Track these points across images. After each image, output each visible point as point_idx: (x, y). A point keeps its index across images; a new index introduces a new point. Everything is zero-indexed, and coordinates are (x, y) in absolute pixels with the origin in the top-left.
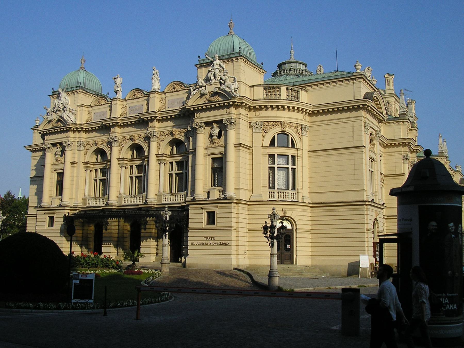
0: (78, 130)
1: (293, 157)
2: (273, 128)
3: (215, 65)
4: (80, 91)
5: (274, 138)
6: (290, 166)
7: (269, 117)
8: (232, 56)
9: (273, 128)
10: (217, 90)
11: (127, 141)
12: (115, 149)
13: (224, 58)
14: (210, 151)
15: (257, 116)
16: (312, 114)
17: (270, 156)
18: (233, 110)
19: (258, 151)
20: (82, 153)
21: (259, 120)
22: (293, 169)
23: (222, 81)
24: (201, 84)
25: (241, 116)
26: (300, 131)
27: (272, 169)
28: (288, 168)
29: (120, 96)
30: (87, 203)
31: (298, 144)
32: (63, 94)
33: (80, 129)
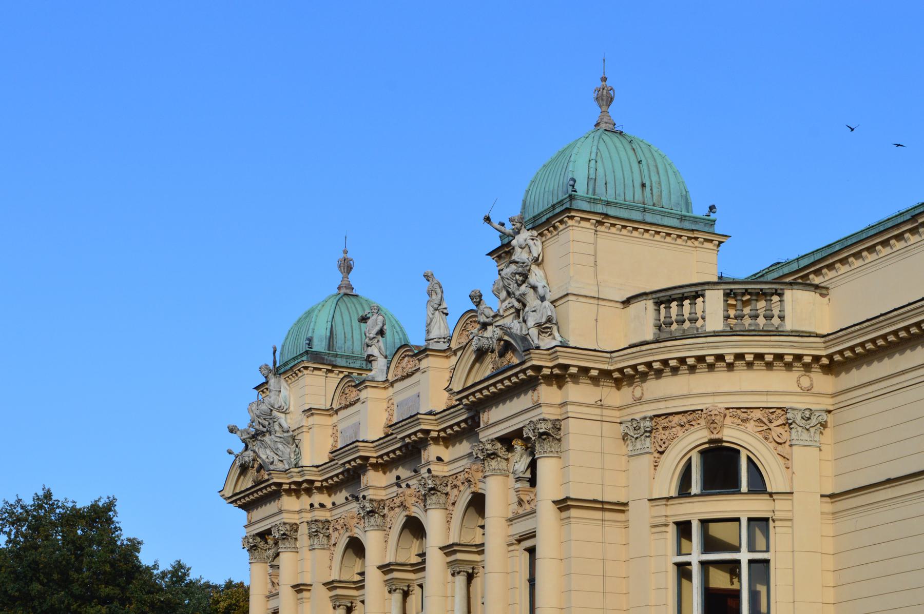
1: (760, 523)
2: (681, 434)
6: (744, 556)
9: (681, 434)
15: (638, 401)
16: (832, 367)
17: (678, 524)
18: (547, 393)
19: (641, 514)
21: (640, 412)
22: (761, 568)
25: (570, 408)
26: (776, 431)
27: (683, 570)
28: (738, 562)
31: (775, 480)
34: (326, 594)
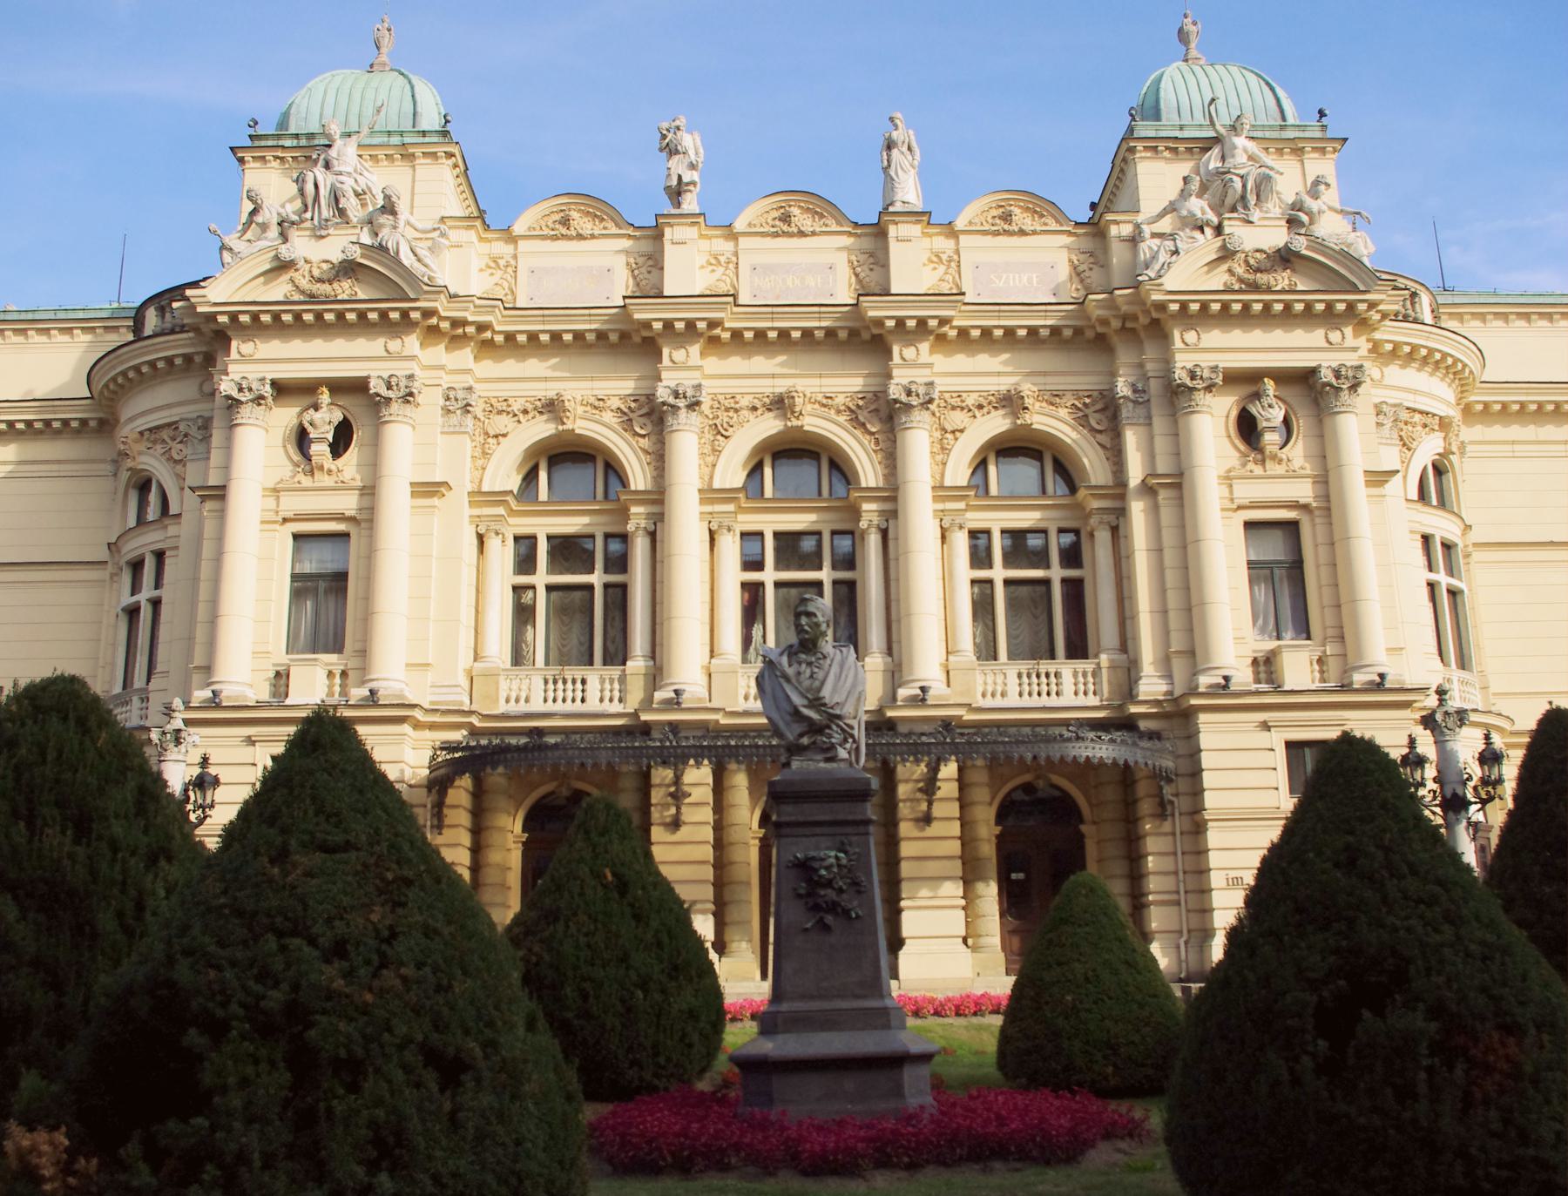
0: (456, 333)
3: (1239, 152)
4: (450, 155)
5: (1425, 469)
7: (1415, 392)
8: (1290, 134)
10: (1300, 244)
11: (745, 413)
12: (687, 442)
13: (1259, 134)
14: (1247, 491)
20: (467, 446)
23: (1305, 218)
24: (1199, 215)
29: (690, 203)
30: (503, 695)
32: (346, 154)
33: (471, 330)
34: (468, 511)
